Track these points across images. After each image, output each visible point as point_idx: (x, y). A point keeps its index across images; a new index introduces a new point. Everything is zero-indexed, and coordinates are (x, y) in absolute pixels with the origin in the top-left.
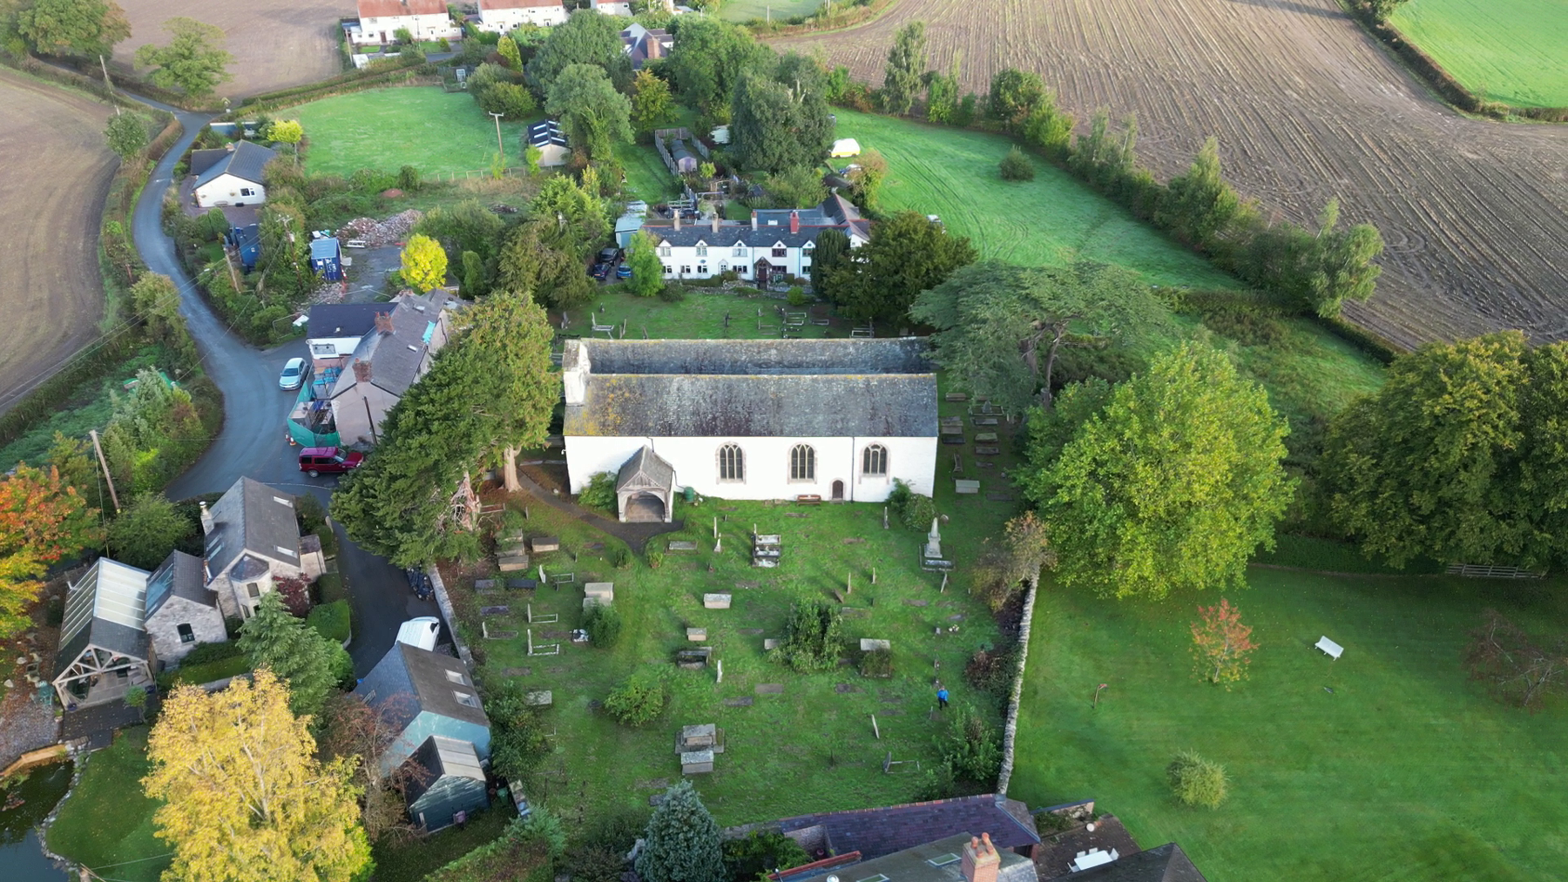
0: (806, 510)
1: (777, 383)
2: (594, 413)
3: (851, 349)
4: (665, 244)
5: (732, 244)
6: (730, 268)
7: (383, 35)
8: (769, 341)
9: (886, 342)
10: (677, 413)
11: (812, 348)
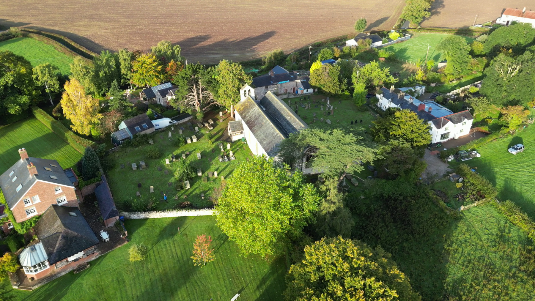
4: (382, 95)
7: (508, 22)
8: (291, 114)
11: (295, 122)
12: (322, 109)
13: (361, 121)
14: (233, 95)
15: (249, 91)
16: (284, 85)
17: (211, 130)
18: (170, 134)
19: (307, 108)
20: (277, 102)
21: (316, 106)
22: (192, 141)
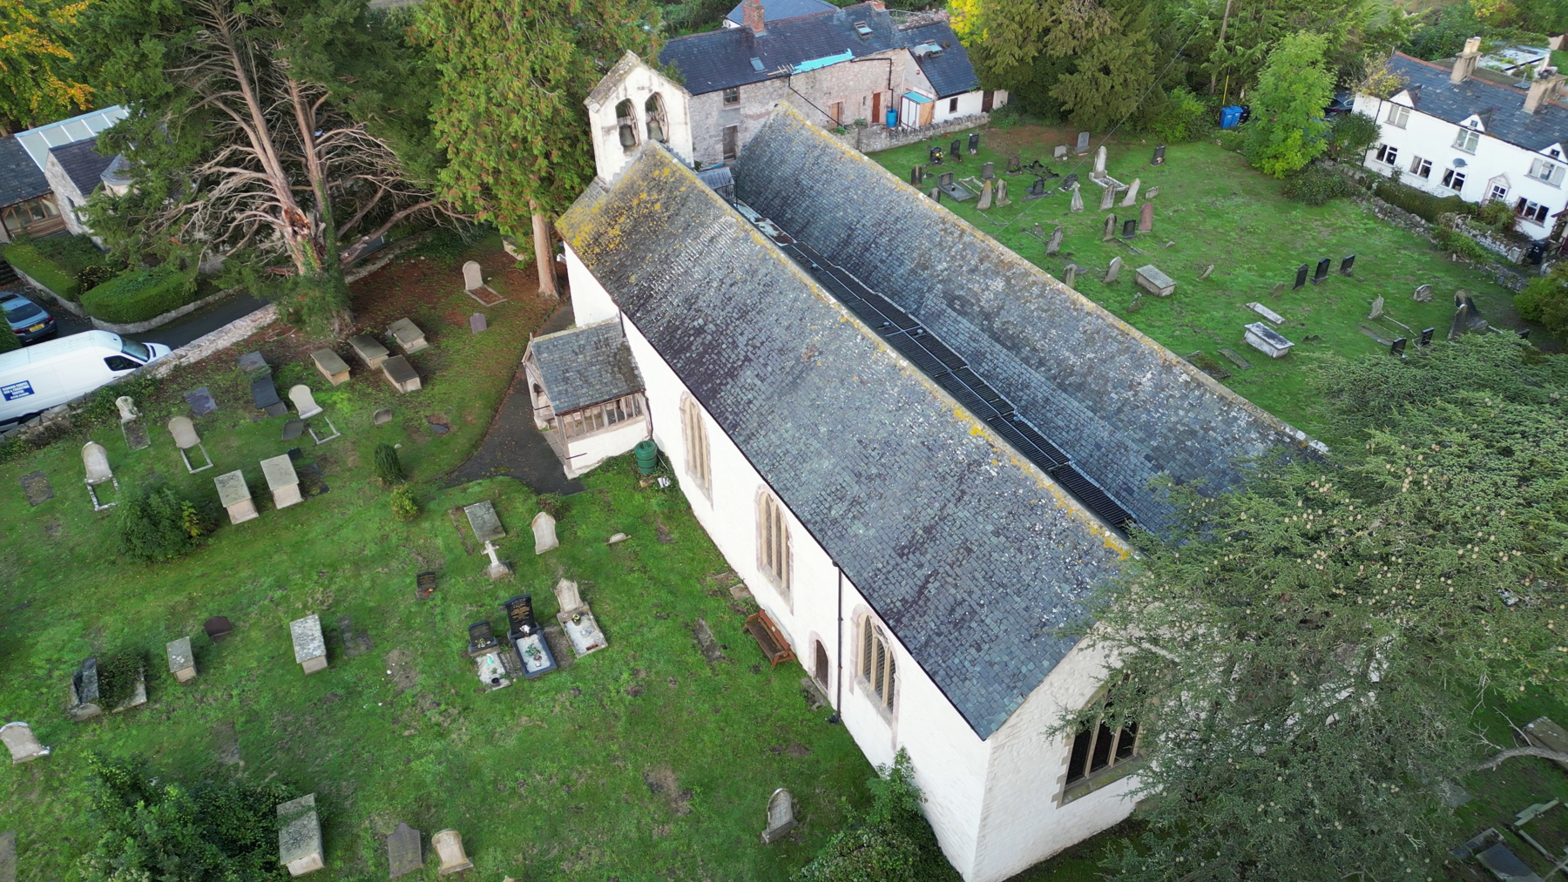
0: (746, 646)
1: (837, 331)
2: (607, 212)
3: (1146, 379)
4: (1404, 98)
5: (1536, 148)
6: (1511, 199)
9: (1244, 413)
10: (675, 282)
12: (1077, 203)
13: (1347, 263)
14: (538, 147)
15: (653, 104)
16: (827, 81)
17: (405, 399)
18: (96, 461)
19: (985, 203)
20: (862, 177)
21: (1037, 189)
22: (260, 494)
